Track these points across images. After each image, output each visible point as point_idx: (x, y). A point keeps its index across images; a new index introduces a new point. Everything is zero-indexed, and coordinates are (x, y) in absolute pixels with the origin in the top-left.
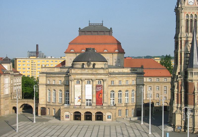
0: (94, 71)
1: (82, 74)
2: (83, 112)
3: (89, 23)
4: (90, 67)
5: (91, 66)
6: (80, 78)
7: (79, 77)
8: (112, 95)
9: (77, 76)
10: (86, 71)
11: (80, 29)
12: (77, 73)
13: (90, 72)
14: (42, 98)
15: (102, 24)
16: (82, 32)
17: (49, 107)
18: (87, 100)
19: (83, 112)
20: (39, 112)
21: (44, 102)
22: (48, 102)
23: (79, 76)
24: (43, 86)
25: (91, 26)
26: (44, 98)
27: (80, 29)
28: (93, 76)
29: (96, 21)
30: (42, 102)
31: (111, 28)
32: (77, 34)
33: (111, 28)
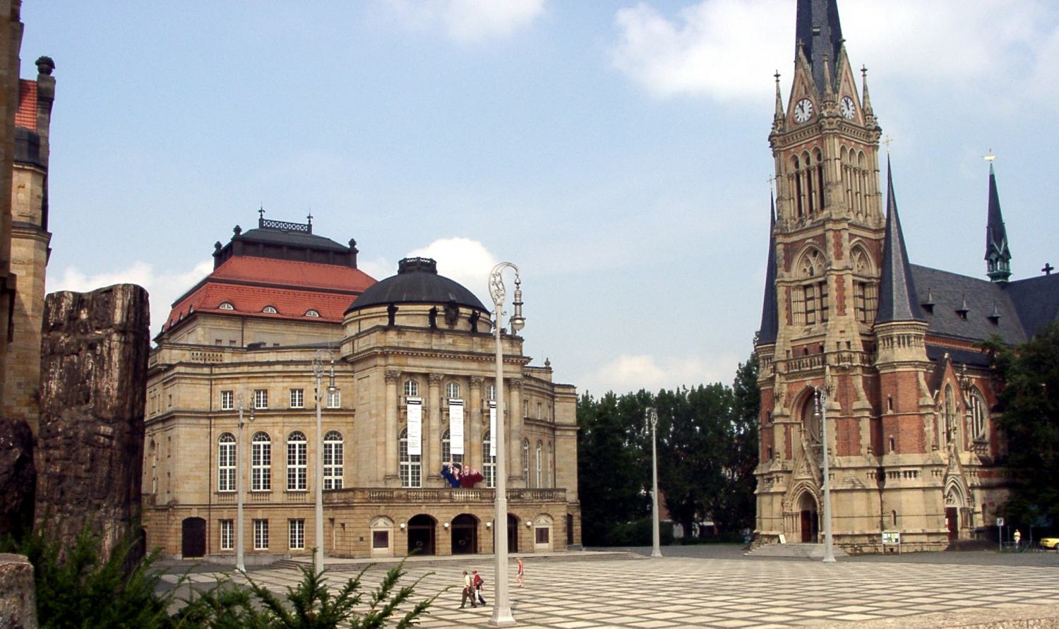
1: (432, 353)
2: (444, 518)
3: (261, 220)
4: (457, 328)
5: (459, 323)
6: (423, 371)
8: (413, 478)
9: (411, 361)
10: (447, 342)
11: (238, 230)
12: (411, 346)
13: (463, 345)
14: (188, 477)
15: (310, 226)
19: (444, 518)
21: (196, 492)
22: (218, 493)
23: (417, 362)
24: (194, 421)
25: (266, 227)
27: (238, 230)
28: (474, 366)
29: (288, 212)
31: (353, 243)
33: (353, 243)
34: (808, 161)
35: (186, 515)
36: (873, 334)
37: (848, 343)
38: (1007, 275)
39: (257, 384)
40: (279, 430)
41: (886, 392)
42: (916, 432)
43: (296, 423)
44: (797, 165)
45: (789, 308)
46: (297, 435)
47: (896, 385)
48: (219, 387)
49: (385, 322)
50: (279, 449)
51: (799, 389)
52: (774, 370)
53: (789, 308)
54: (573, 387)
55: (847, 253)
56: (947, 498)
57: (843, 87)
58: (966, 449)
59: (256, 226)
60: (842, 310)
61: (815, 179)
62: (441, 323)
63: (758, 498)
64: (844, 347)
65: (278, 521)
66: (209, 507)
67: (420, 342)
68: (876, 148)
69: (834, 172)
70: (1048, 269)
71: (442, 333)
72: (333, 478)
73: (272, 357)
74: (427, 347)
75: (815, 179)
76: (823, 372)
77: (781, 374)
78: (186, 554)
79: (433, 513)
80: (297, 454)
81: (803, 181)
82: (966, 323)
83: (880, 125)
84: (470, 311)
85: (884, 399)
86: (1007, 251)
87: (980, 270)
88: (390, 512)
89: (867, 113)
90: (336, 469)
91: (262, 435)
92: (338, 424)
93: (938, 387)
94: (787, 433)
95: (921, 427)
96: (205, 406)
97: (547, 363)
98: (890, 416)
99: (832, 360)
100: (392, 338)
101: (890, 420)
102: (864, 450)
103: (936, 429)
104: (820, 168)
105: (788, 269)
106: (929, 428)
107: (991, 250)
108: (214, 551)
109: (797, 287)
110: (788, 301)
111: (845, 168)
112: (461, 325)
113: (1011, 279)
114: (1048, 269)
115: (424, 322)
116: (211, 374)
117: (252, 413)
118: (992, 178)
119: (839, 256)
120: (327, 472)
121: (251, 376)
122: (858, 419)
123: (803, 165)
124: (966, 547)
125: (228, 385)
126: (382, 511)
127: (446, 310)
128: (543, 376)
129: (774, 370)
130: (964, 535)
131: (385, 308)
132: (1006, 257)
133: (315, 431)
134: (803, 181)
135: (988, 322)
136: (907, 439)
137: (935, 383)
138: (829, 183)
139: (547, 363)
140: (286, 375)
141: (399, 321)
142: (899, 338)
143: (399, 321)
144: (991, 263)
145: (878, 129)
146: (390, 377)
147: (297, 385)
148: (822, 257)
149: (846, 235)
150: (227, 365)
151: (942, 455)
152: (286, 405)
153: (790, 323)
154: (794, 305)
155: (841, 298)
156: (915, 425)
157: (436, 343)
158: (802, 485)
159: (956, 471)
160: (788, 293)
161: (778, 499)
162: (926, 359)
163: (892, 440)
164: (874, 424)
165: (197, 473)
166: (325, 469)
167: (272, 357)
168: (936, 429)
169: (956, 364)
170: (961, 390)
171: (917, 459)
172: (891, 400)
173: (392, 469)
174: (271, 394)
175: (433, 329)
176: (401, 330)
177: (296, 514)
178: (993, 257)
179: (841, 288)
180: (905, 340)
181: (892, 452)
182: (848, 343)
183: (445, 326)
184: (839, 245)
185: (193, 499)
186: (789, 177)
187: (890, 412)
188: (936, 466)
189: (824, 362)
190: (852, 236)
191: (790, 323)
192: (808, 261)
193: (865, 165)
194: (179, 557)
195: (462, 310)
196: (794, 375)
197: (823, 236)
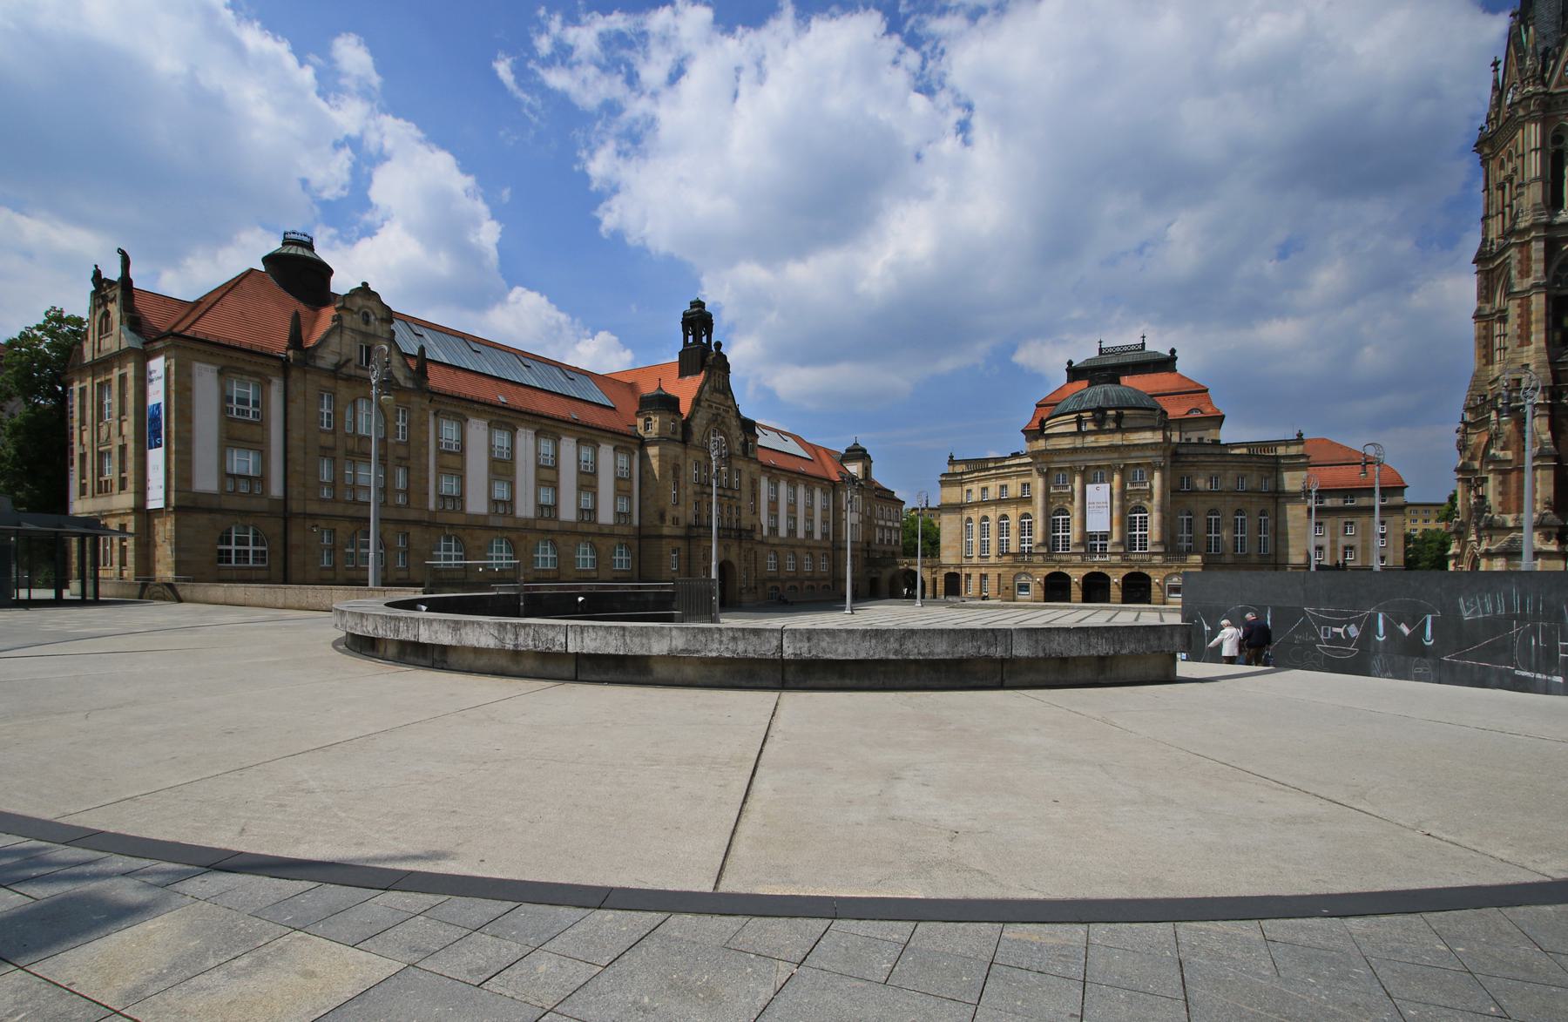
0: (1117, 439)
2: (1076, 576)
10: (1090, 441)
11: (1070, 363)
13: (1104, 440)
16: (1074, 373)
17: (967, 571)
18: (1093, 536)
19: (1076, 576)
20: (941, 587)
30: (948, 556)
31: (1173, 351)
32: (1063, 377)
33: (1173, 351)
35: (946, 571)
39: (983, 484)
40: (993, 514)
43: (1002, 510)
46: (1005, 517)
48: (966, 487)
50: (993, 526)
55: (1538, 268)
60: (1524, 339)
62: (1090, 426)
65: (993, 575)
66: (960, 566)
67: (1065, 443)
80: (1003, 529)
97: (1300, 435)
115: (1074, 428)
128: (1293, 450)
139: (1300, 435)
140: (997, 477)
154: (1497, 340)
155: (1525, 325)
157: (1078, 442)
185: (953, 561)
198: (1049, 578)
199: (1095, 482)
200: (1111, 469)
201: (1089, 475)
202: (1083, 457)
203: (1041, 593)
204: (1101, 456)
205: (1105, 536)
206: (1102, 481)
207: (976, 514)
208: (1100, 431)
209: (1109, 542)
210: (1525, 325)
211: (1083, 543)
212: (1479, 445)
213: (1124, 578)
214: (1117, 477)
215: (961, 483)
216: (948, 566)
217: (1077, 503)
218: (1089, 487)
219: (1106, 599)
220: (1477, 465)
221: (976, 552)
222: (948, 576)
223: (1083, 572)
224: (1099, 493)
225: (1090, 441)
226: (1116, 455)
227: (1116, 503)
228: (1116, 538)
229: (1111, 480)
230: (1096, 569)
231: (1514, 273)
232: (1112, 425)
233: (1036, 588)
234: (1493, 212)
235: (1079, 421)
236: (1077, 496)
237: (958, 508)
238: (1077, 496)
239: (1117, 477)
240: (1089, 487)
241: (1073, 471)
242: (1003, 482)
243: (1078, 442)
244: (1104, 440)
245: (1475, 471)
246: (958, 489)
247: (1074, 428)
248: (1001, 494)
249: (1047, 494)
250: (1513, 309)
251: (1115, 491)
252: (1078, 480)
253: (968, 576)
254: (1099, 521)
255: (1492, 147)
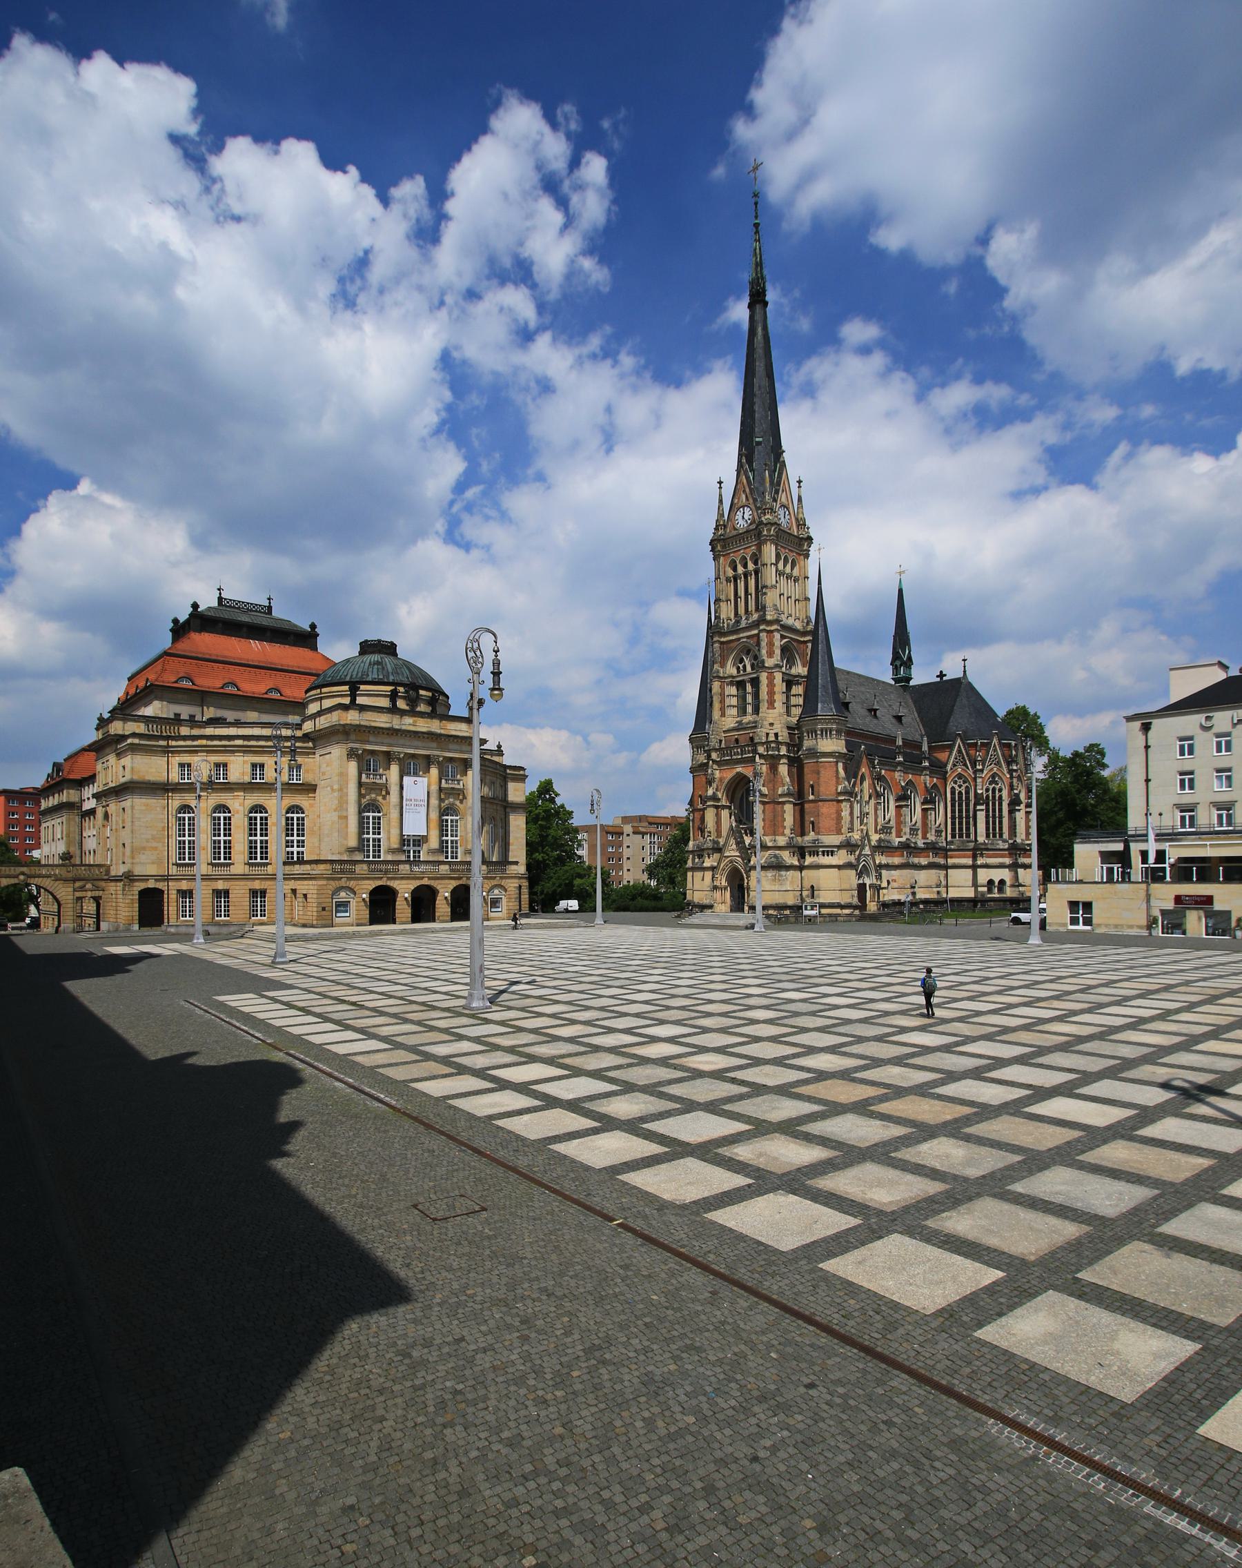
2: (404, 890)
3: (220, 599)
6: (384, 749)
7: (382, 744)
10: (408, 723)
11: (195, 606)
13: (423, 725)
14: (144, 848)
15: (270, 608)
18: (404, 841)
19: (404, 890)
22: (178, 865)
26: (156, 848)
27: (195, 606)
31: (313, 626)
33: (313, 626)
34: (745, 566)
35: (142, 886)
36: (798, 726)
37: (776, 735)
38: (908, 679)
40: (239, 804)
41: (809, 780)
42: (834, 816)
44: (735, 569)
45: (722, 701)
47: (818, 773)
48: (176, 760)
49: (347, 701)
51: (729, 774)
52: (709, 757)
53: (722, 701)
54: (523, 769)
55: (778, 652)
56: (860, 875)
57: (783, 498)
58: (876, 832)
59: (215, 604)
60: (771, 704)
61: (752, 583)
62: (401, 704)
63: (689, 874)
64: (772, 738)
65: (239, 893)
66: (167, 878)
67: (382, 721)
68: (807, 556)
69: (770, 575)
70: (941, 675)
71: (402, 713)
72: (295, 849)
73: (232, 731)
74: (387, 725)
75: (752, 583)
76: (752, 760)
77: (714, 761)
78: (141, 925)
79: (394, 884)
81: (741, 585)
82: (875, 721)
83: (812, 535)
84: (430, 694)
85: (806, 786)
86: (910, 658)
87: (887, 676)
88: (352, 884)
89: (801, 524)
90: (298, 841)
91: (222, 808)
92: (300, 800)
93: (855, 777)
94: (718, 816)
95: (839, 812)
96: (162, 777)
97: (499, 746)
98: (812, 801)
99: (761, 750)
100: (352, 717)
101: (812, 805)
102: (787, 831)
103: (851, 814)
104: (757, 572)
105: (723, 665)
106: (845, 814)
107: (896, 656)
108: (173, 922)
109: (731, 683)
110: (722, 695)
111: (780, 573)
112: (422, 708)
113: (912, 683)
114: (941, 675)
115: (385, 702)
116: (168, 746)
117: (210, 786)
118: (900, 591)
119: (771, 654)
120: (289, 844)
121: (210, 751)
122: (783, 803)
123: (740, 570)
124: (874, 918)
125: (186, 759)
126: (343, 883)
127: (406, 692)
128: (496, 759)
129: (709, 757)
130: (872, 907)
131: (347, 688)
132: (908, 663)
133: (276, 805)
134: (741, 585)
135: (894, 721)
136: (826, 822)
137: (852, 773)
138: (766, 587)
139: (499, 746)
140: (246, 750)
141: (360, 700)
142: (822, 730)
143: (360, 700)
144: (896, 669)
145: (810, 539)
146: (351, 754)
147: (258, 759)
148: (756, 658)
149: (777, 636)
150: (185, 738)
151: (856, 836)
152: (247, 779)
153: (723, 715)
154: (727, 700)
155: (771, 693)
156: (833, 810)
157: (396, 722)
158: (731, 862)
159: (867, 851)
160: (722, 688)
161: (709, 874)
162: (845, 751)
163: (813, 823)
164: (797, 808)
165: (154, 844)
166: (287, 842)
167: (232, 731)
168: (851, 814)
169: (870, 755)
170: (873, 779)
171: (835, 840)
172: (812, 787)
173: (353, 842)
174: (231, 767)
175: (393, 710)
176: (363, 708)
177: (257, 885)
178: (898, 663)
179: (771, 684)
180: (826, 732)
181: (812, 833)
182: (776, 735)
183: (407, 708)
184: (771, 644)
185: (152, 870)
186: (728, 580)
187: (811, 797)
188: (849, 846)
189: (755, 751)
190: (783, 637)
191: (723, 715)
192: (742, 661)
193: (796, 572)
194: (136, 927)
195: (422, 692)
196: (727, 763)
197: (758, 635)
198: (374, 893)
199: (409, 774)
200: (428, 761)
201: (411, 766)
202: (401, 741)
203: (366, 913)
204: (419, 743)
205: (419, 841)
206: (416, 774)
207: (205, 805)
208: (413, 713)
209: (424, 848)
210: (771, 693)
211: (400, 850)
212: (721, 779)
213: (453, 892)
214: (434, 771)
215: (167, 751)
216: (145, 878)
217: (394, 797)
218: (406, 779)
219: (431, 918)
220: (719, 795)
221: (204, 856)
222: (144, 894)
223: (413, 885)
224: (418, 788)
225: (408, 723)
226: (434, 745)
227: (434, 802)
228: (434, 843)
229: (427, 771)
230: (425, 882)
231: (764, 652)
232: (428, 709)
233: (358, 907)
234: (723, 597)
235: (393, 696)
236: (394, 790)
237: (163, 788)
238: (394, 790)
239: (434, 771)
240: (406, 779)
241: (388, 757)
242: (258, 759)
243: (396, 722)
244: (423, 725)
245: (718, 800)
246: (160, 761)
247: (385, 702)
248: (254, 776)
249: (360, 784)
250: (764, 677)
251: (434, 788)
252: (394, 769)
253: (186, 894)
254: (416, 824)
255: (724, 547)
